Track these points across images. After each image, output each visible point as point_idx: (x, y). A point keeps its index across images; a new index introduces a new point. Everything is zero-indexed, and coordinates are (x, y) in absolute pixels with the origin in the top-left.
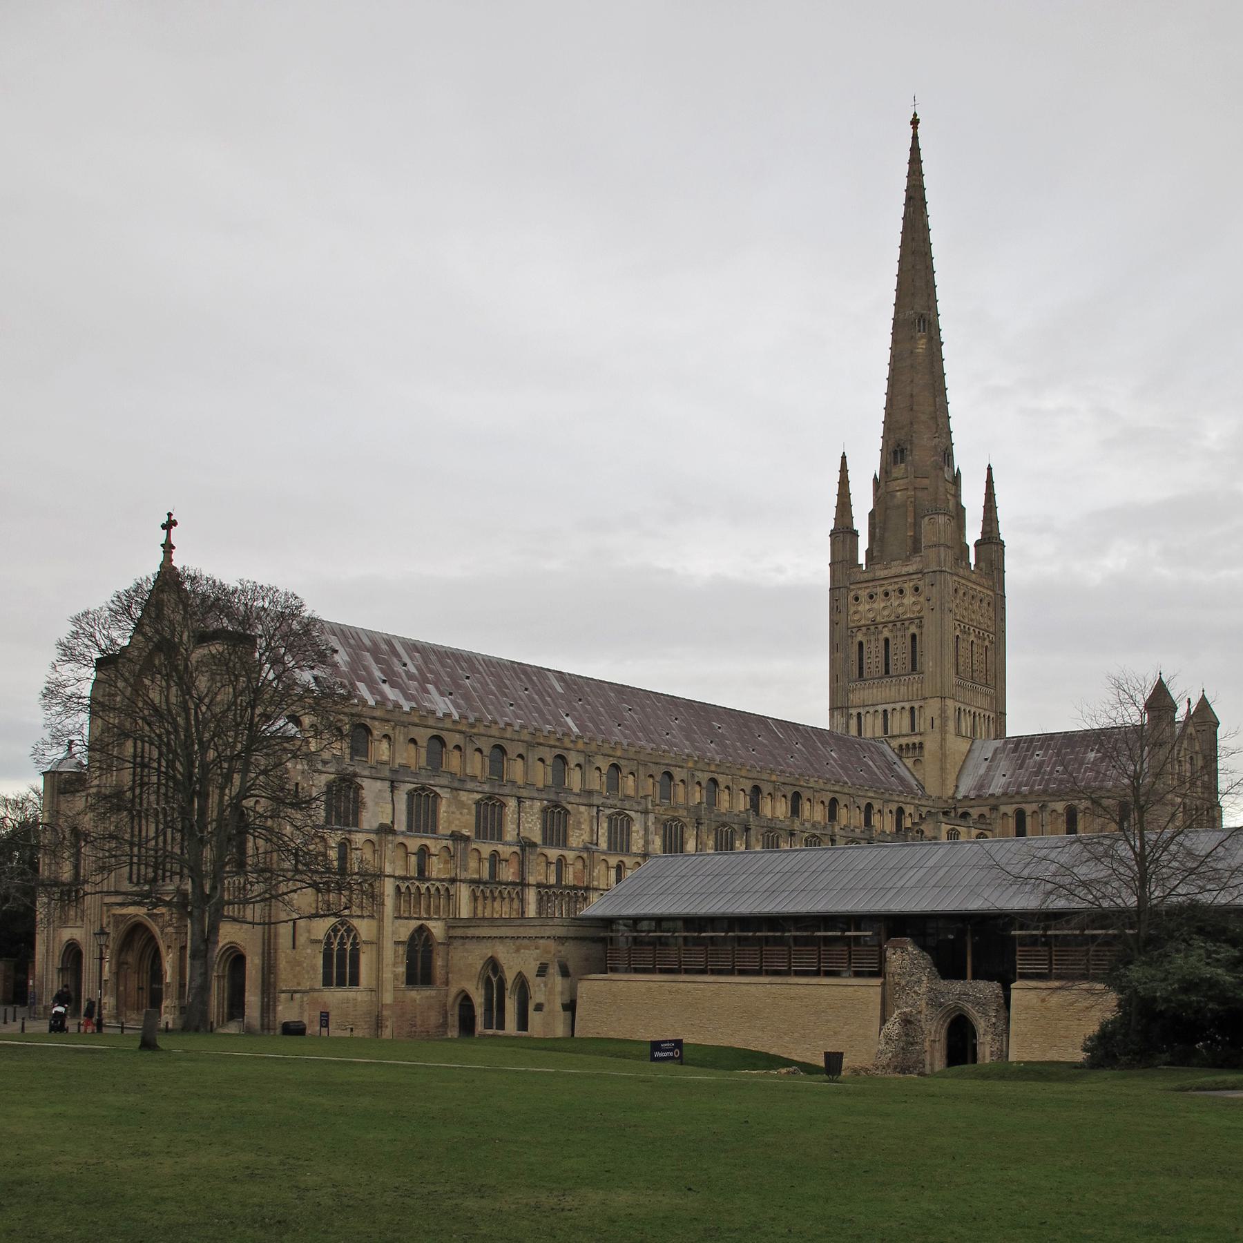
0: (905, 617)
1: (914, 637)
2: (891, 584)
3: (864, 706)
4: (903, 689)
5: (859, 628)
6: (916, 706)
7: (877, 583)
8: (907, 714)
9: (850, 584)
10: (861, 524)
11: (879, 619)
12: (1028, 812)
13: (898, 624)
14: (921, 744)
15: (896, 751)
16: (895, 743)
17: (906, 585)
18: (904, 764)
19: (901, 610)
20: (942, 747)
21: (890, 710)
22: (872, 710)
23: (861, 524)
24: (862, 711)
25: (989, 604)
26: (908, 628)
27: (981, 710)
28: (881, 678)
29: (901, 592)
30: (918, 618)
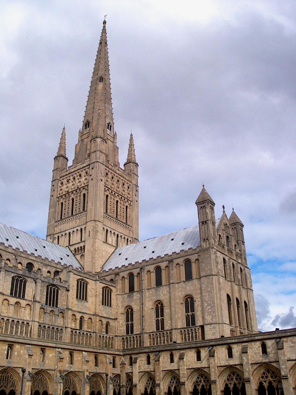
0: (81, 187)
1: (84, 195)
2: (76, 174)
3: (60, 232)
4: (78, 221)
5: (62, 197)
6: (83, 228)
7: (71, 175)
8: (79, 232)
9: (60, 178)
10: (71, 155)
11: (70, 190)
12: (135, 274)
13: (78, 191)
14: (84, 246)
15: (73, 252)
16: (72, 248)
17: (82, 173)
18: (76, 258)
19: (79, 184)
20: (93, 246)
21: (71, 232)
22: (64, 234)
23: (71, 155)
24: (60, 235)
25: (128, 188)
26: (82, 191)
27: (122, 235)
28: (69, 217)
29: (80, 176)
30: (86, 186)
